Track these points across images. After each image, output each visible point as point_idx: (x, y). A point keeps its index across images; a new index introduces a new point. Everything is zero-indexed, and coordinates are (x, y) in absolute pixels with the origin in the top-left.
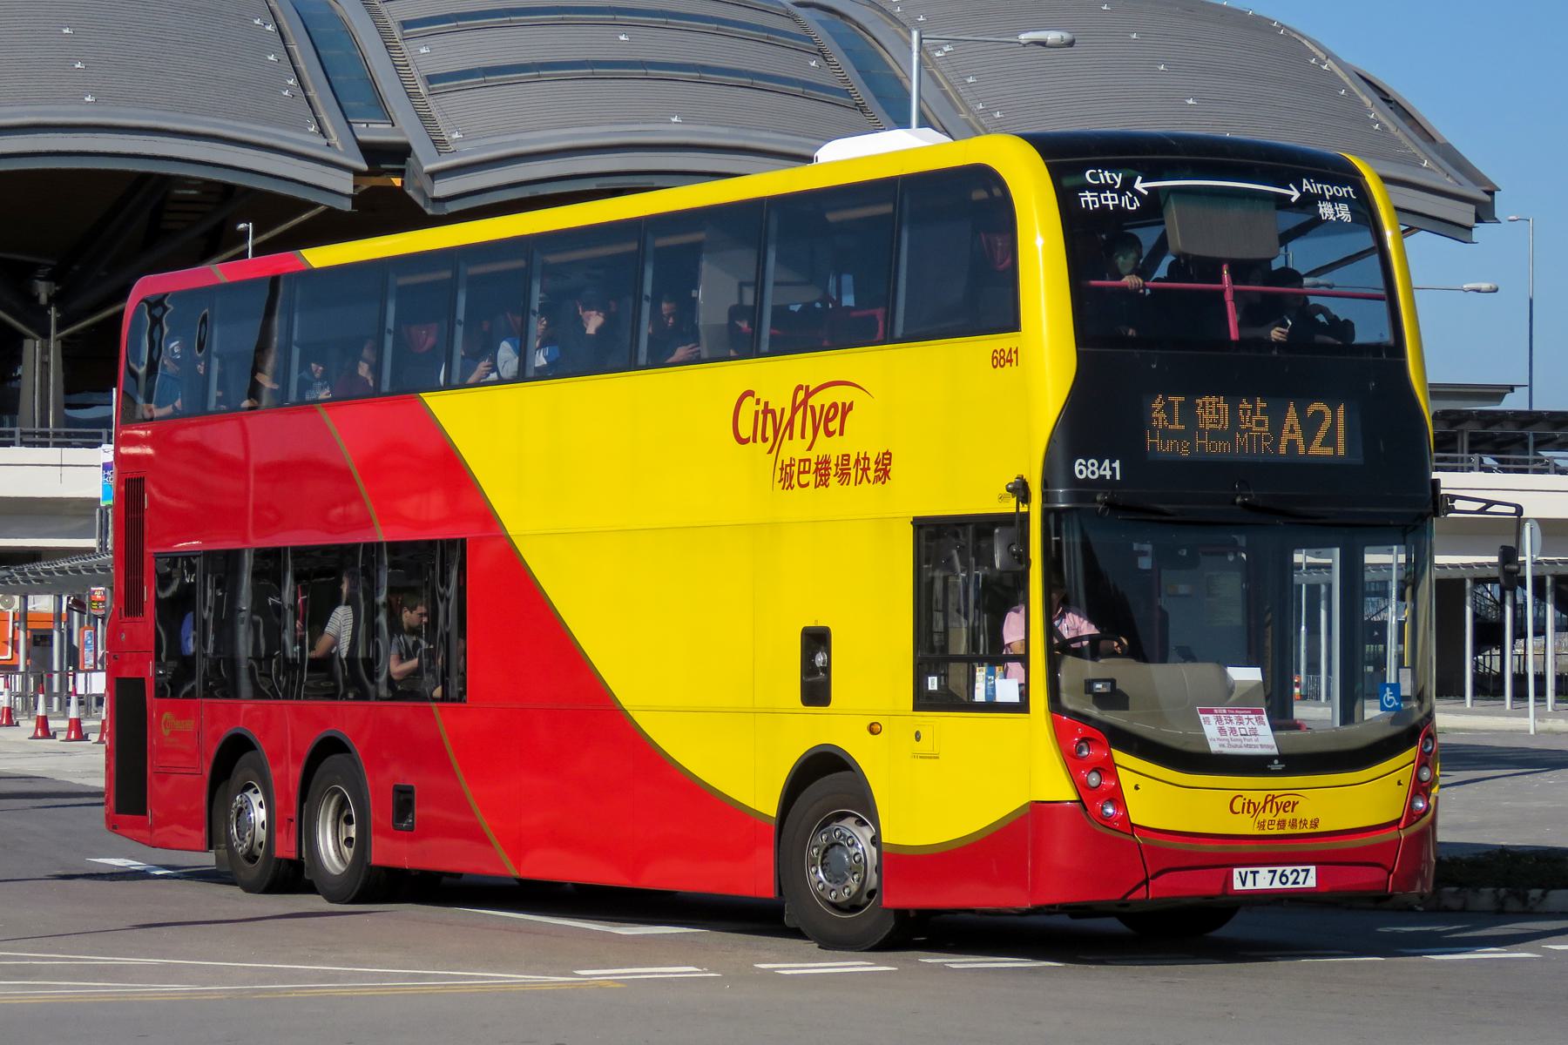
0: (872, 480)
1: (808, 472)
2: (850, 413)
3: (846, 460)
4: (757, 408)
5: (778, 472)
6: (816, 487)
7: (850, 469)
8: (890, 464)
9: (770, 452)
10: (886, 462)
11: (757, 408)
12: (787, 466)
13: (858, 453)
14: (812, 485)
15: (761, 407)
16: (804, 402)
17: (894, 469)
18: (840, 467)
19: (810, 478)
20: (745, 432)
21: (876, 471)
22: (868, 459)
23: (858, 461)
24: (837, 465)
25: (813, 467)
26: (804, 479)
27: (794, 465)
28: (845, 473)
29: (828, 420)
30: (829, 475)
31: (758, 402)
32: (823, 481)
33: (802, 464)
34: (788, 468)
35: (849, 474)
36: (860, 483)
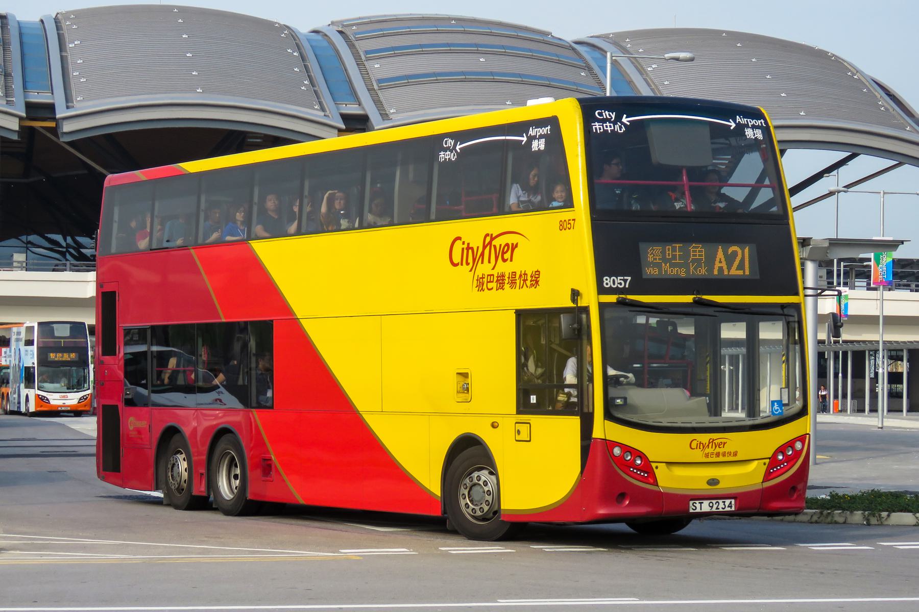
0: (529, 285)
1: (493, 282)
2: (516, 250)
3: (514, 275)
4: (463, 246)
5: (475, 282)
6: (497, 290)
7: (516, 280)
8: (539, 277)
9: (471, 271)
10: (536, 276)
11: (463, 246)
12: (480, 278)
13: (521, 271)
15: (465, 246)
16: (490, 243)
17: (541, 280)
18: (510, 279)
19: (494, 285)
20: (456, 259)
21: (531, 281)
22: (527, 274)
23: (520, 276)
24: (509, 278)
25: (495, 279)
26: (490, 285)
27: (484, 278)
28: (514, 282)
29: (503, 253)
30: (504, 283)
31: (464, 243)
32: (501, 286)
33: (489, 277)
34: (481, 281)
35: (516, 283)
36: (522, 287)
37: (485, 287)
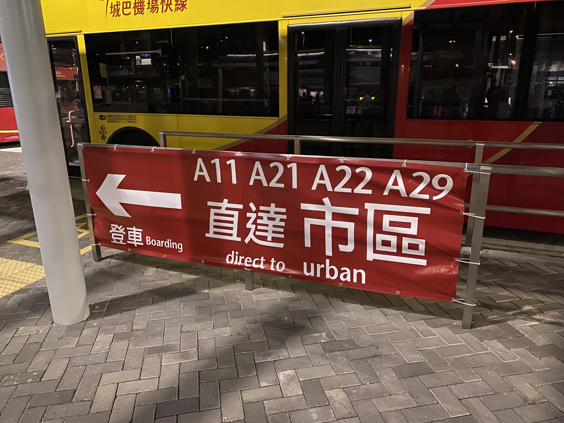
0: (174, 9)
1: (130, 8)
5: (109, 9)
7: (158, 5)
12: (115, 6)
14: (133, 13)
18: (151, 4)
19: (132, 10)
21: (176, 5)
24: (149, 3)
25: (133, 5)
26: (126, 11)
27: (120, 5)
30: (144, 8)
34: (116, 7)
35: (158, 8)
37: (121, 12)
